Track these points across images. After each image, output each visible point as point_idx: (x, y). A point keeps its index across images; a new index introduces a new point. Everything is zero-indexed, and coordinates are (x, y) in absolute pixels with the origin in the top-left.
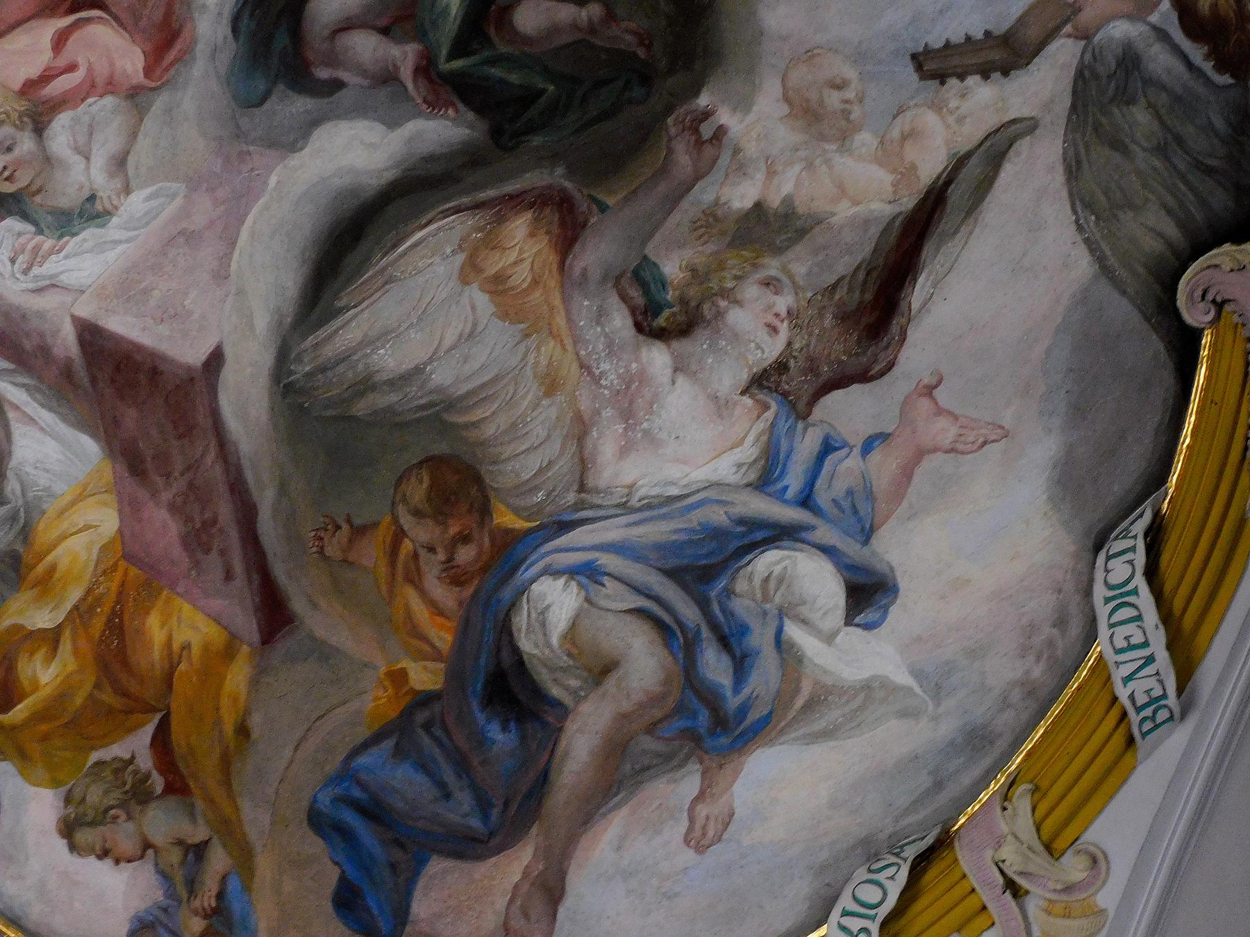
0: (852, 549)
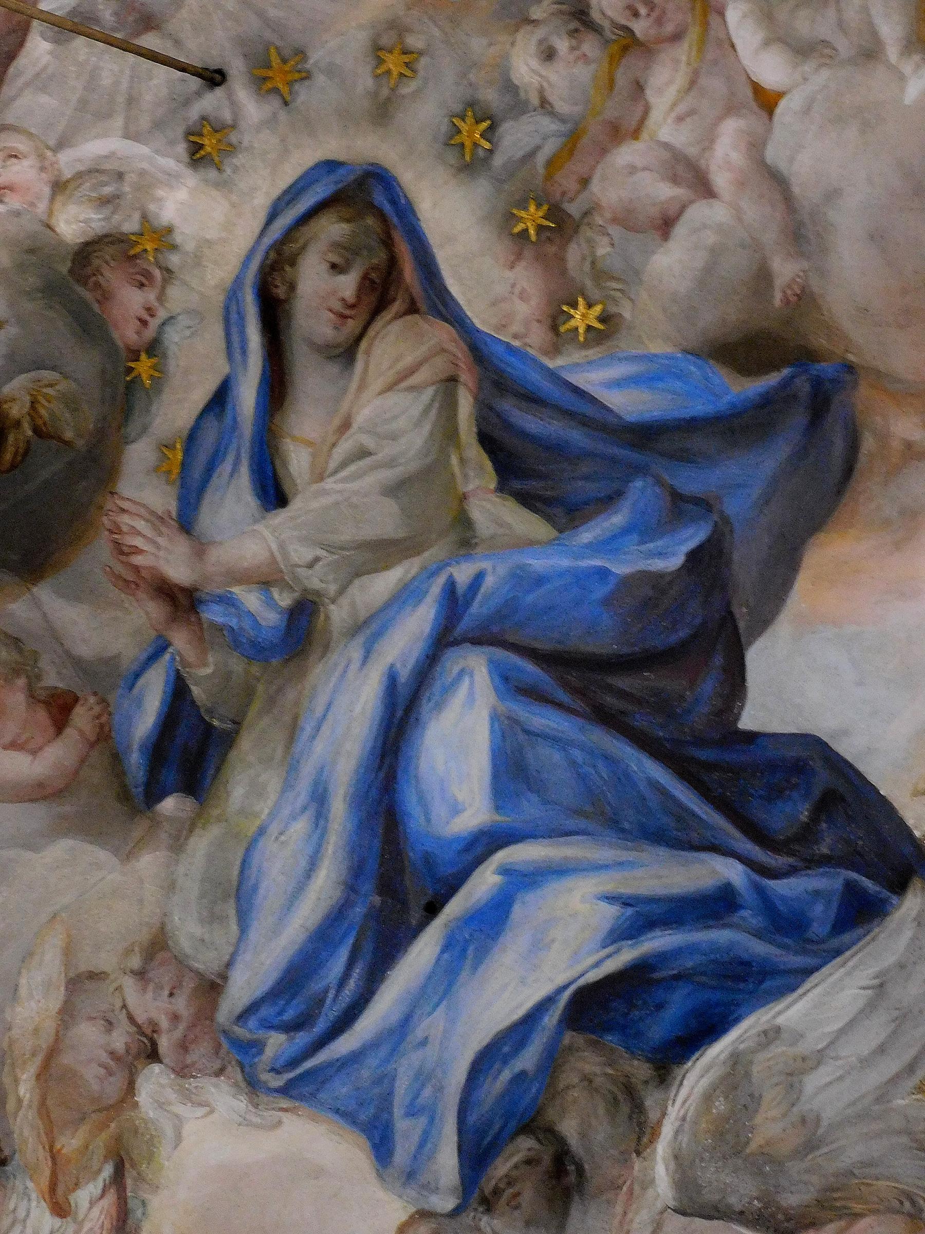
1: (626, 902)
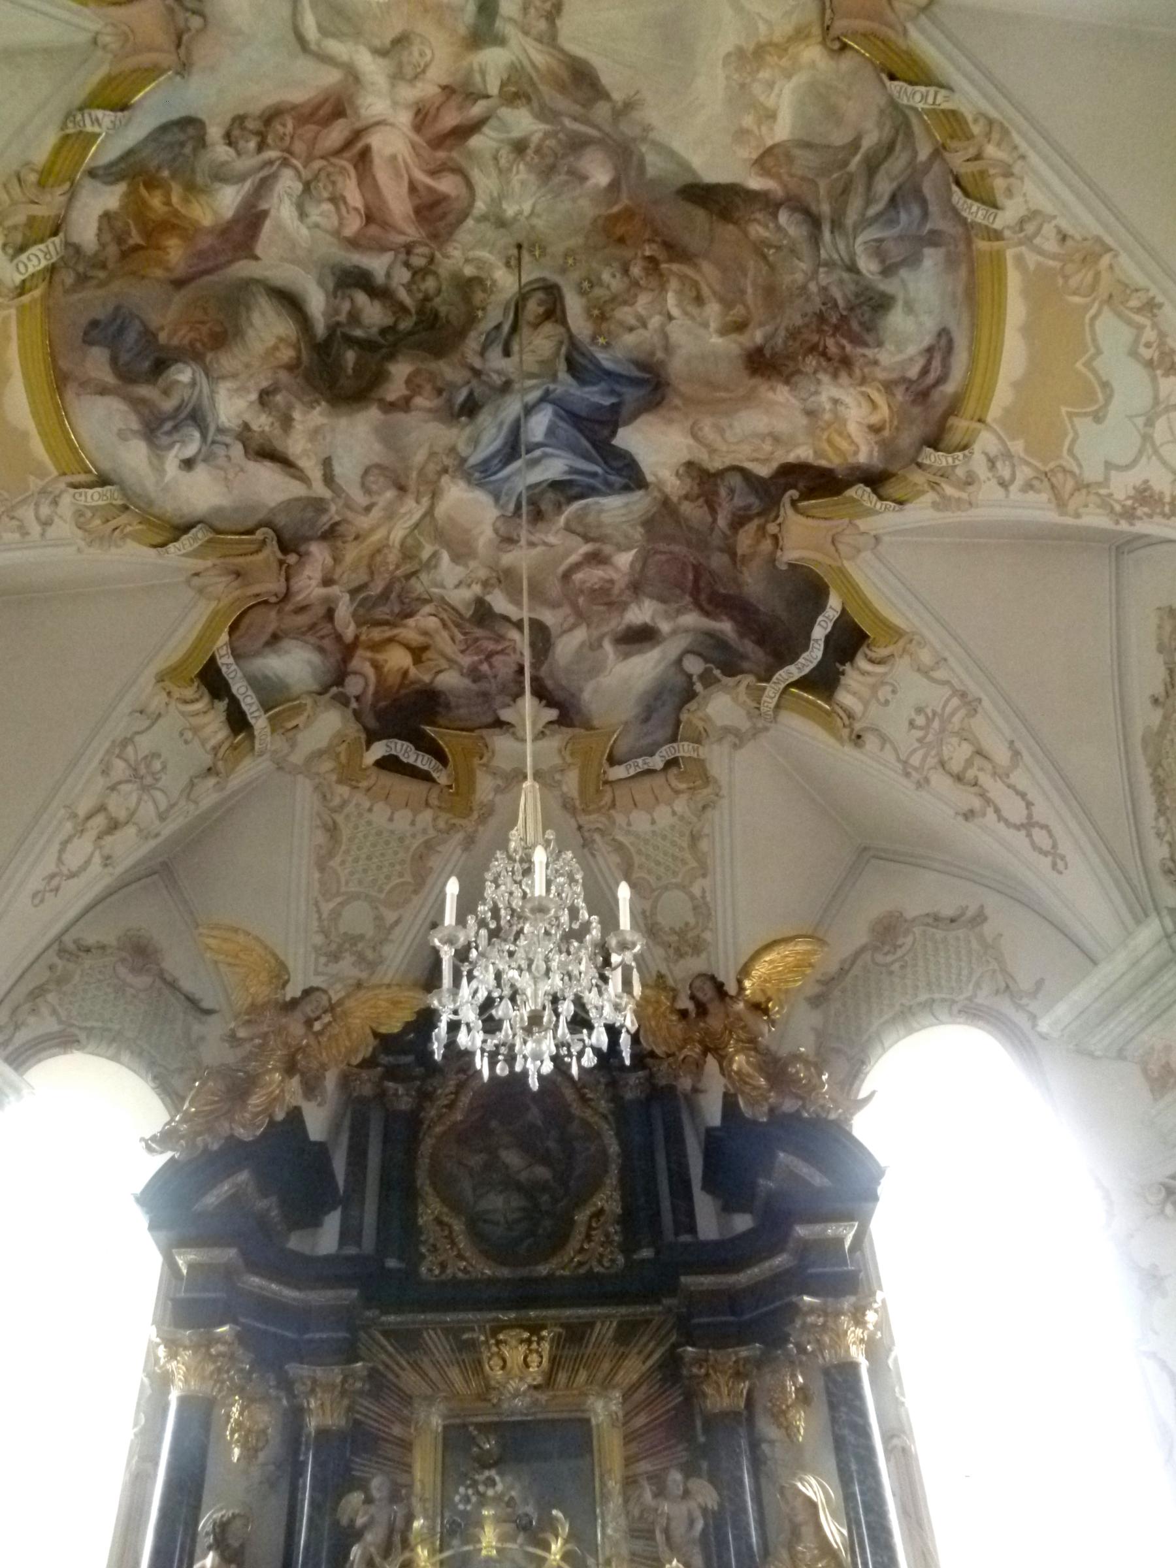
0: (200, 457)
1: (571, 467)
